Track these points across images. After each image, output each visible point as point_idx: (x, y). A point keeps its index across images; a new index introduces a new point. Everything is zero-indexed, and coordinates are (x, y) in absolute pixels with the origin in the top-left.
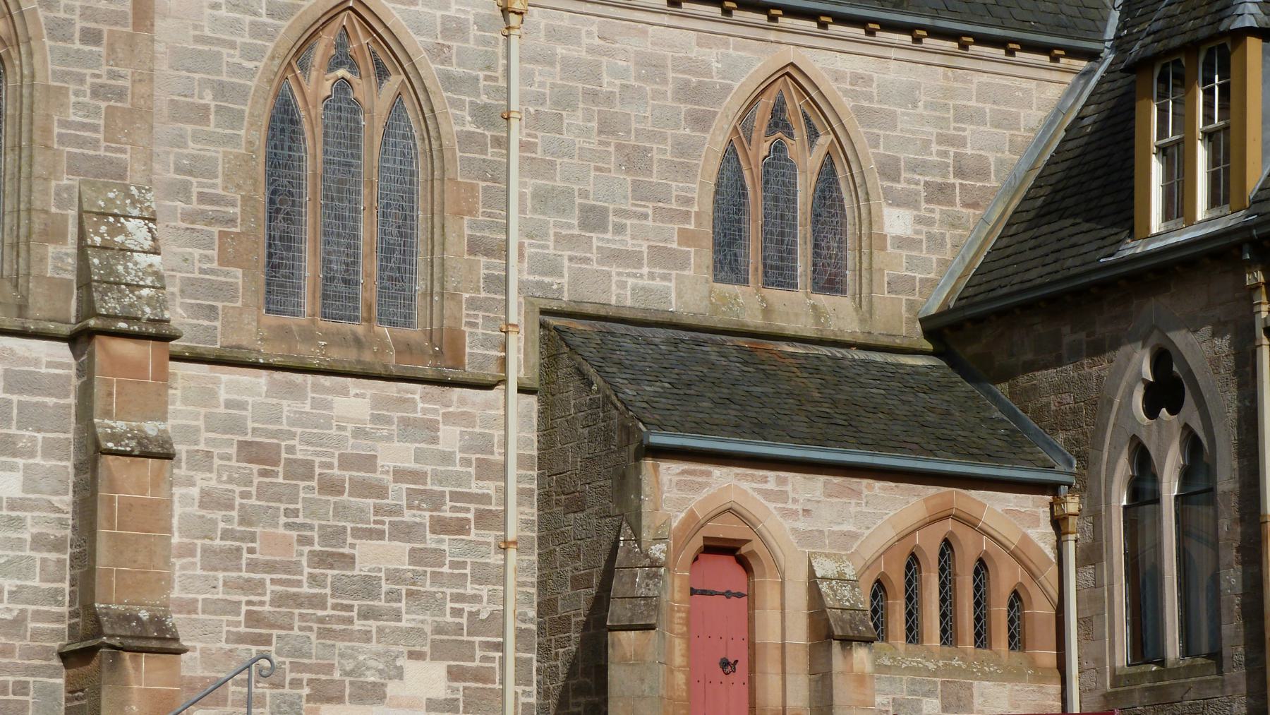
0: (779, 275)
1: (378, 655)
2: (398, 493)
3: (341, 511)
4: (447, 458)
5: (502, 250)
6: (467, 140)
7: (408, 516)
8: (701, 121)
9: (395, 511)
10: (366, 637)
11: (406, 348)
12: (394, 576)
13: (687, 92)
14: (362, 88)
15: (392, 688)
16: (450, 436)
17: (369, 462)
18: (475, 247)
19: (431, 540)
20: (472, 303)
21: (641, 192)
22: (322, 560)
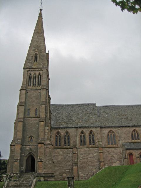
0: (136, 139)
5: (120, 140)
14: (112, 134)
16: (118, 150)
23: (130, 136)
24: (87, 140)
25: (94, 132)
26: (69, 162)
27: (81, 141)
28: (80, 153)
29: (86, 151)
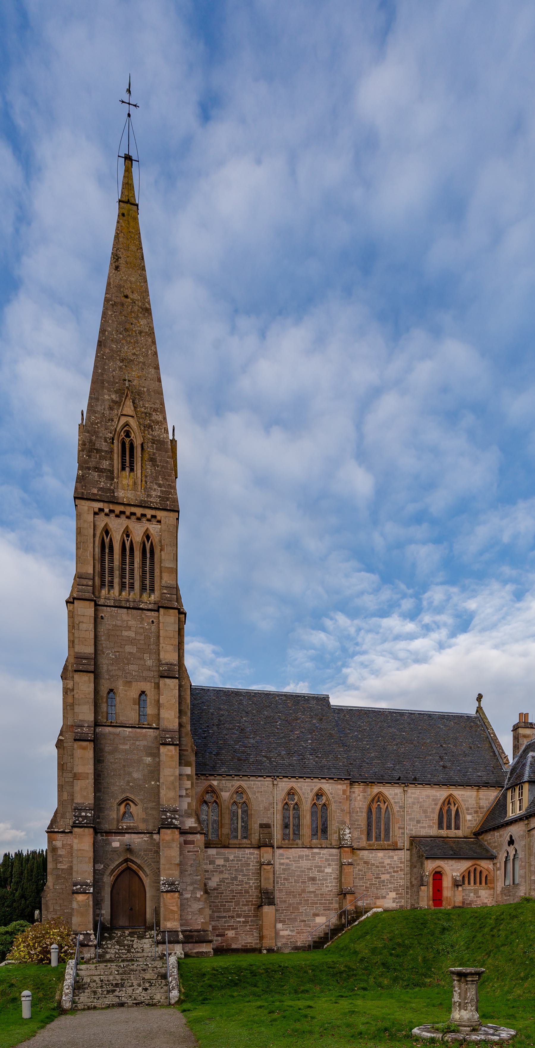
0: (449, 828)
1: (385, 892)
2: (388, 867)
3: (379, 870)
4: (395, 861)
6: (398, 811)
7: (389, 871)
8: (436, 804)
9: (387, 870)
10: (383, 889)
11: (389, 845)
12: (387, 880)
13: (433, 800)
15: (387, 896)
16: (396, 858)
17: (383, 863)
18: (399, 828)
19: (393, 874)
20: (399, 837)
21: (426, 817)
22: (376, 878)
23: (436, 816)
24: (306, 820)
25: (330, 796)
26: (247, 892)
27: (286, 826)
28: (282, 864)
29: (301, 857)
